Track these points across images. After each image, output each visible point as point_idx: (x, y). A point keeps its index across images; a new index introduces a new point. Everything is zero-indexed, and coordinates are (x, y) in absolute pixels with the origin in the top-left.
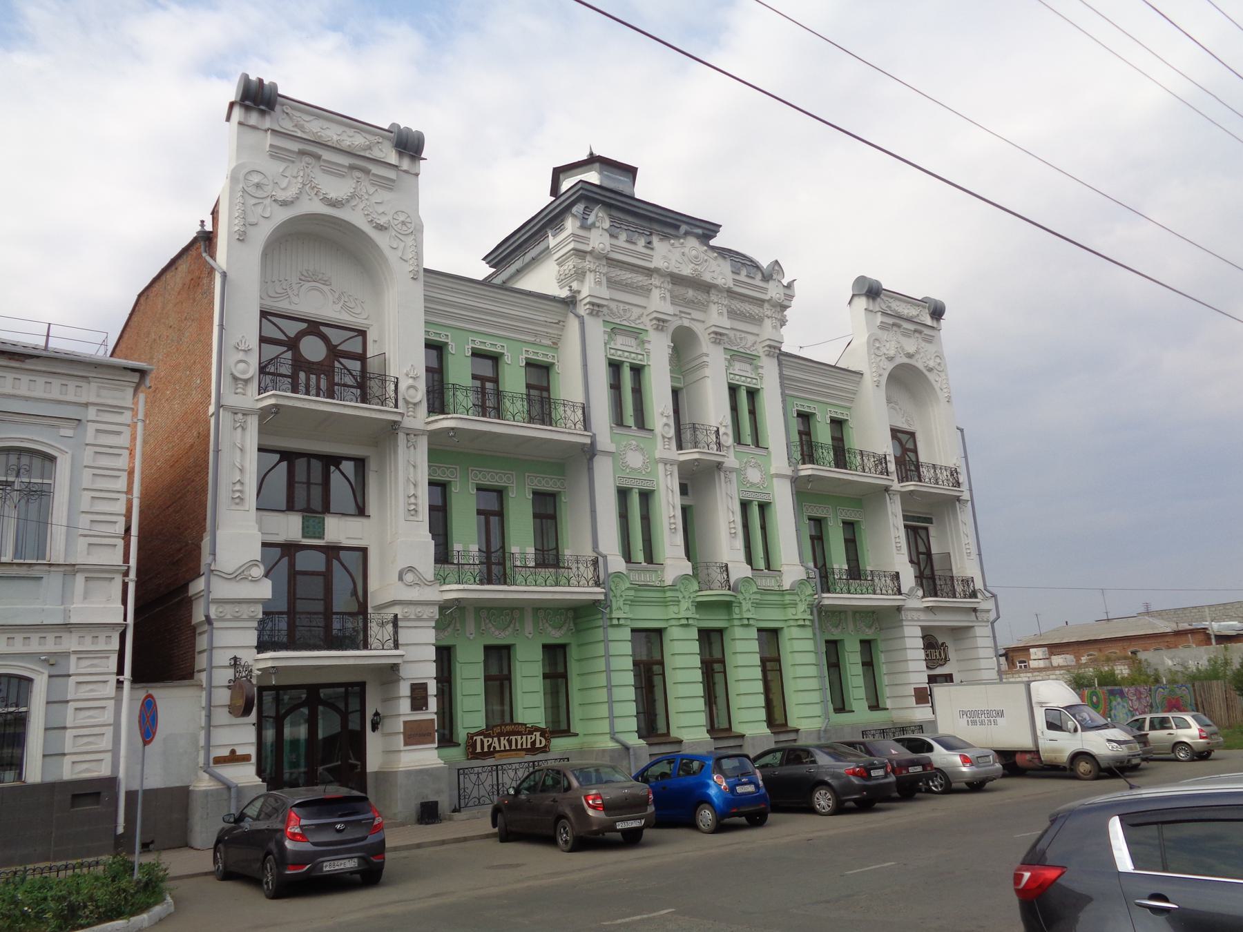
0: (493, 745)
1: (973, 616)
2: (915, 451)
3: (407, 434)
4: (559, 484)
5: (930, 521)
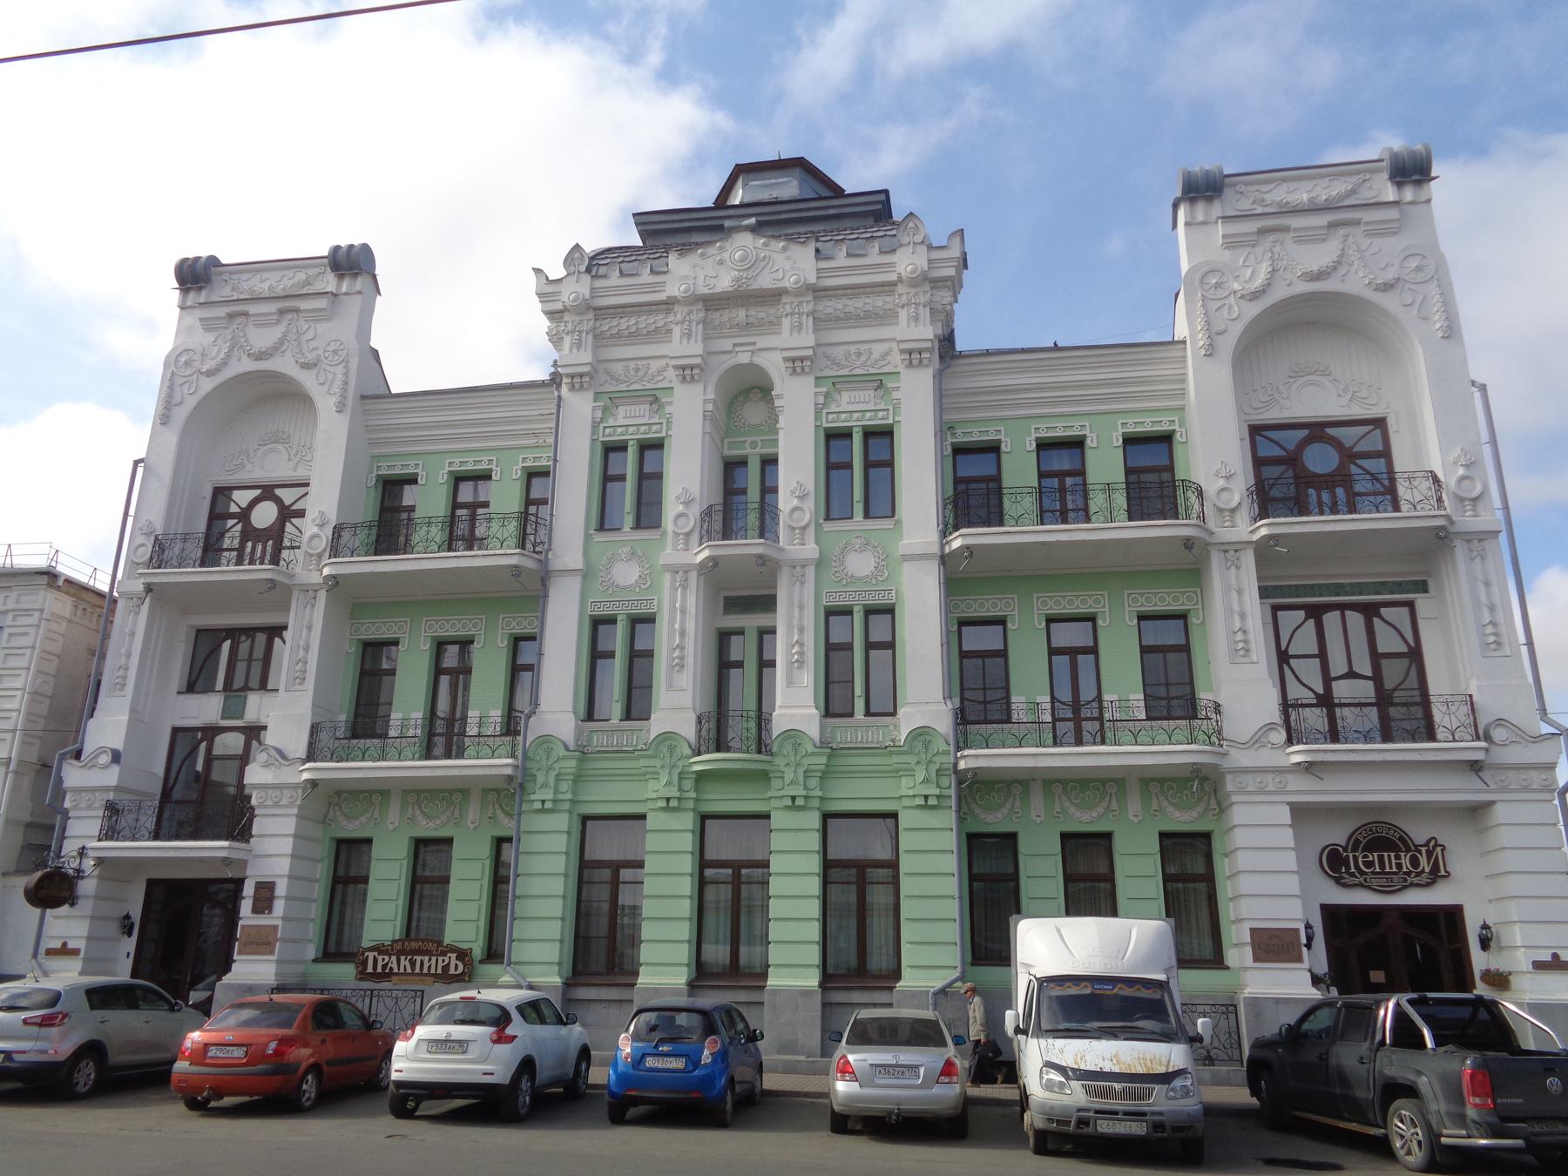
0: (390, 965)
1: (1472, 782)
2: (1386, 454)
5: (1422, 587)
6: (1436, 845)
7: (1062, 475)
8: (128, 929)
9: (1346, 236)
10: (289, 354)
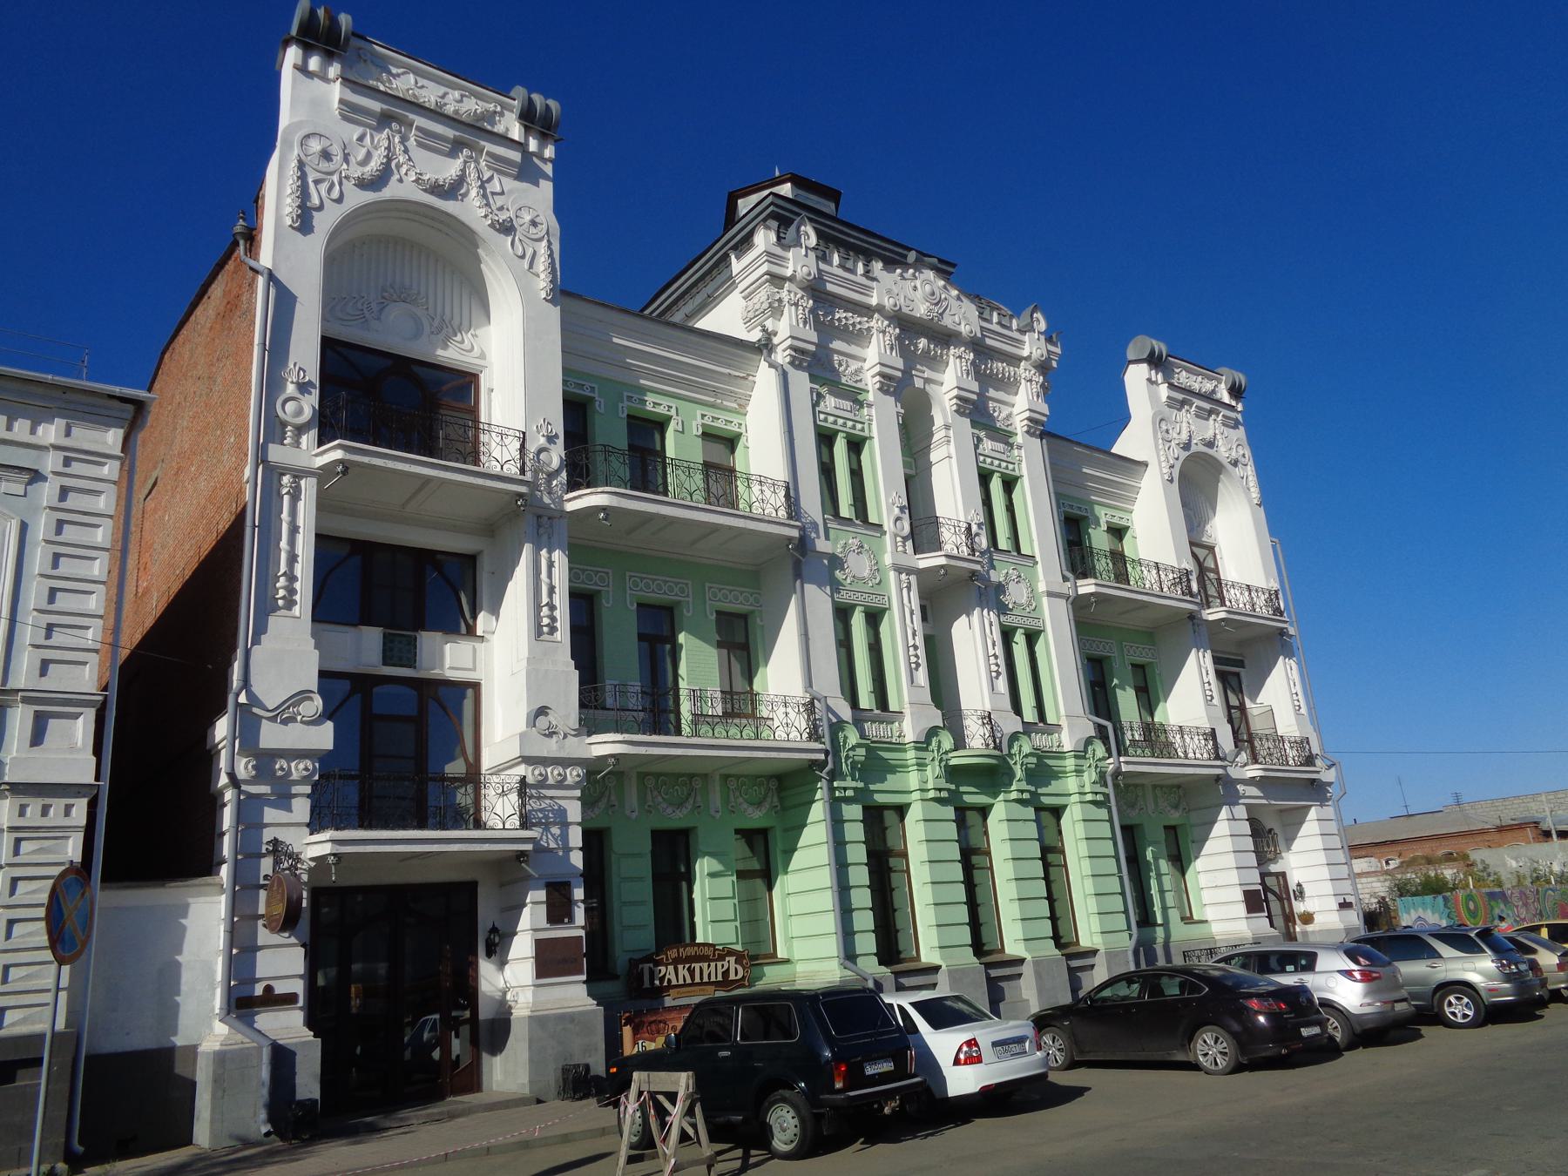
2: (1216, 571)
3: (539, 517)
4: (751, 599)
5: (1241, 664)
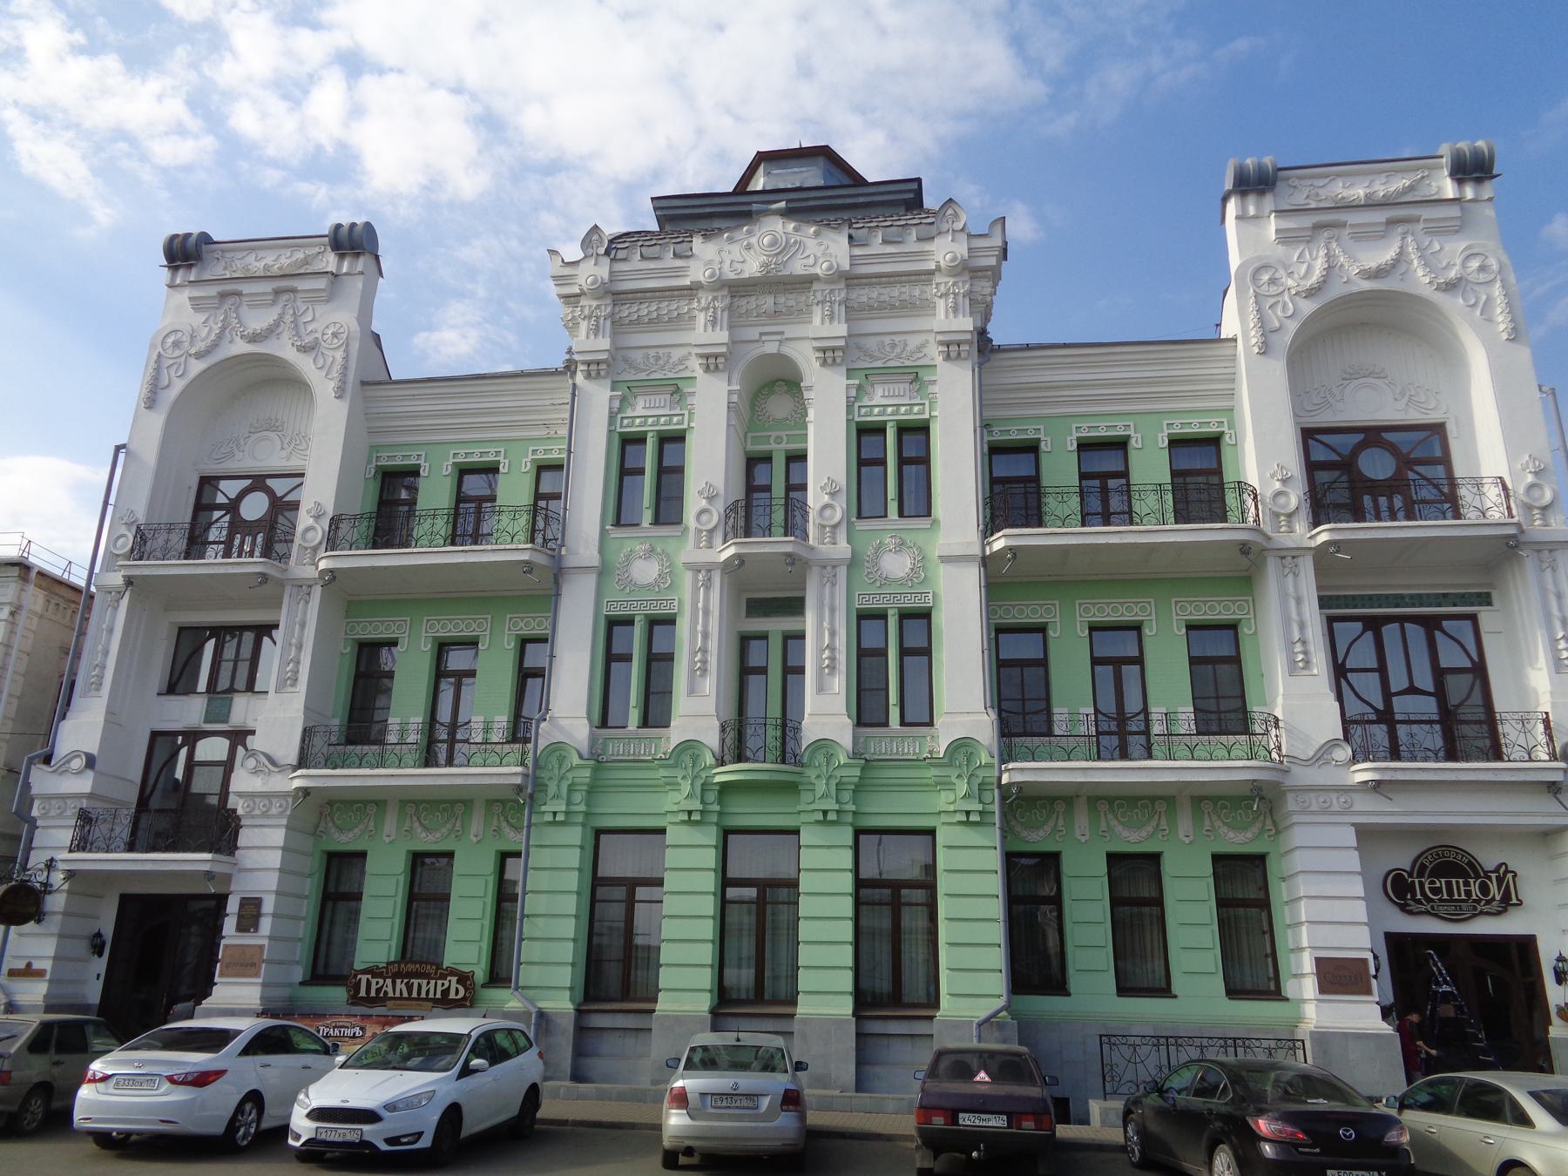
0: (384, 988)
2: (1446, 460)
5: (1486, 599)
6: (1507, 871)
7: (1104, 476)
8: (98, 949)
9: (1405, 234)
10: (286, 335)
